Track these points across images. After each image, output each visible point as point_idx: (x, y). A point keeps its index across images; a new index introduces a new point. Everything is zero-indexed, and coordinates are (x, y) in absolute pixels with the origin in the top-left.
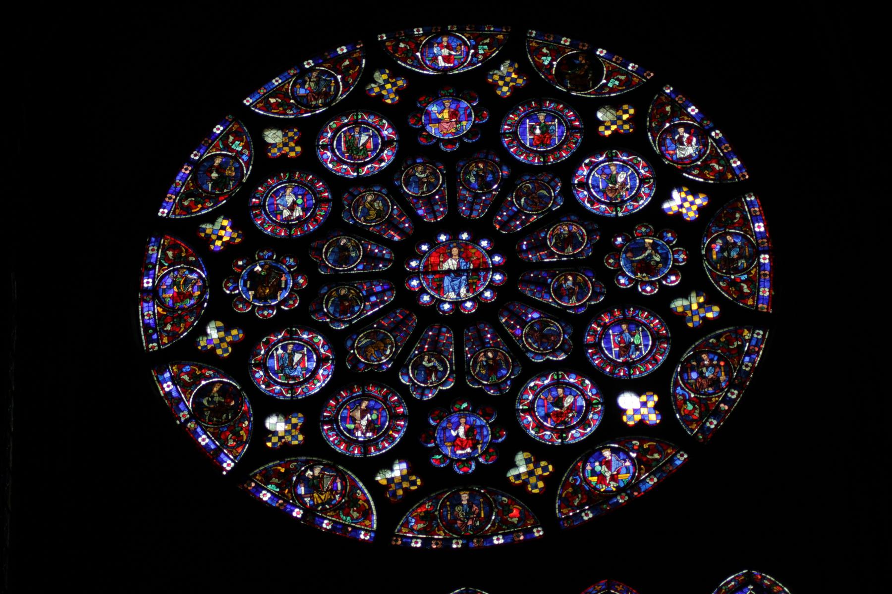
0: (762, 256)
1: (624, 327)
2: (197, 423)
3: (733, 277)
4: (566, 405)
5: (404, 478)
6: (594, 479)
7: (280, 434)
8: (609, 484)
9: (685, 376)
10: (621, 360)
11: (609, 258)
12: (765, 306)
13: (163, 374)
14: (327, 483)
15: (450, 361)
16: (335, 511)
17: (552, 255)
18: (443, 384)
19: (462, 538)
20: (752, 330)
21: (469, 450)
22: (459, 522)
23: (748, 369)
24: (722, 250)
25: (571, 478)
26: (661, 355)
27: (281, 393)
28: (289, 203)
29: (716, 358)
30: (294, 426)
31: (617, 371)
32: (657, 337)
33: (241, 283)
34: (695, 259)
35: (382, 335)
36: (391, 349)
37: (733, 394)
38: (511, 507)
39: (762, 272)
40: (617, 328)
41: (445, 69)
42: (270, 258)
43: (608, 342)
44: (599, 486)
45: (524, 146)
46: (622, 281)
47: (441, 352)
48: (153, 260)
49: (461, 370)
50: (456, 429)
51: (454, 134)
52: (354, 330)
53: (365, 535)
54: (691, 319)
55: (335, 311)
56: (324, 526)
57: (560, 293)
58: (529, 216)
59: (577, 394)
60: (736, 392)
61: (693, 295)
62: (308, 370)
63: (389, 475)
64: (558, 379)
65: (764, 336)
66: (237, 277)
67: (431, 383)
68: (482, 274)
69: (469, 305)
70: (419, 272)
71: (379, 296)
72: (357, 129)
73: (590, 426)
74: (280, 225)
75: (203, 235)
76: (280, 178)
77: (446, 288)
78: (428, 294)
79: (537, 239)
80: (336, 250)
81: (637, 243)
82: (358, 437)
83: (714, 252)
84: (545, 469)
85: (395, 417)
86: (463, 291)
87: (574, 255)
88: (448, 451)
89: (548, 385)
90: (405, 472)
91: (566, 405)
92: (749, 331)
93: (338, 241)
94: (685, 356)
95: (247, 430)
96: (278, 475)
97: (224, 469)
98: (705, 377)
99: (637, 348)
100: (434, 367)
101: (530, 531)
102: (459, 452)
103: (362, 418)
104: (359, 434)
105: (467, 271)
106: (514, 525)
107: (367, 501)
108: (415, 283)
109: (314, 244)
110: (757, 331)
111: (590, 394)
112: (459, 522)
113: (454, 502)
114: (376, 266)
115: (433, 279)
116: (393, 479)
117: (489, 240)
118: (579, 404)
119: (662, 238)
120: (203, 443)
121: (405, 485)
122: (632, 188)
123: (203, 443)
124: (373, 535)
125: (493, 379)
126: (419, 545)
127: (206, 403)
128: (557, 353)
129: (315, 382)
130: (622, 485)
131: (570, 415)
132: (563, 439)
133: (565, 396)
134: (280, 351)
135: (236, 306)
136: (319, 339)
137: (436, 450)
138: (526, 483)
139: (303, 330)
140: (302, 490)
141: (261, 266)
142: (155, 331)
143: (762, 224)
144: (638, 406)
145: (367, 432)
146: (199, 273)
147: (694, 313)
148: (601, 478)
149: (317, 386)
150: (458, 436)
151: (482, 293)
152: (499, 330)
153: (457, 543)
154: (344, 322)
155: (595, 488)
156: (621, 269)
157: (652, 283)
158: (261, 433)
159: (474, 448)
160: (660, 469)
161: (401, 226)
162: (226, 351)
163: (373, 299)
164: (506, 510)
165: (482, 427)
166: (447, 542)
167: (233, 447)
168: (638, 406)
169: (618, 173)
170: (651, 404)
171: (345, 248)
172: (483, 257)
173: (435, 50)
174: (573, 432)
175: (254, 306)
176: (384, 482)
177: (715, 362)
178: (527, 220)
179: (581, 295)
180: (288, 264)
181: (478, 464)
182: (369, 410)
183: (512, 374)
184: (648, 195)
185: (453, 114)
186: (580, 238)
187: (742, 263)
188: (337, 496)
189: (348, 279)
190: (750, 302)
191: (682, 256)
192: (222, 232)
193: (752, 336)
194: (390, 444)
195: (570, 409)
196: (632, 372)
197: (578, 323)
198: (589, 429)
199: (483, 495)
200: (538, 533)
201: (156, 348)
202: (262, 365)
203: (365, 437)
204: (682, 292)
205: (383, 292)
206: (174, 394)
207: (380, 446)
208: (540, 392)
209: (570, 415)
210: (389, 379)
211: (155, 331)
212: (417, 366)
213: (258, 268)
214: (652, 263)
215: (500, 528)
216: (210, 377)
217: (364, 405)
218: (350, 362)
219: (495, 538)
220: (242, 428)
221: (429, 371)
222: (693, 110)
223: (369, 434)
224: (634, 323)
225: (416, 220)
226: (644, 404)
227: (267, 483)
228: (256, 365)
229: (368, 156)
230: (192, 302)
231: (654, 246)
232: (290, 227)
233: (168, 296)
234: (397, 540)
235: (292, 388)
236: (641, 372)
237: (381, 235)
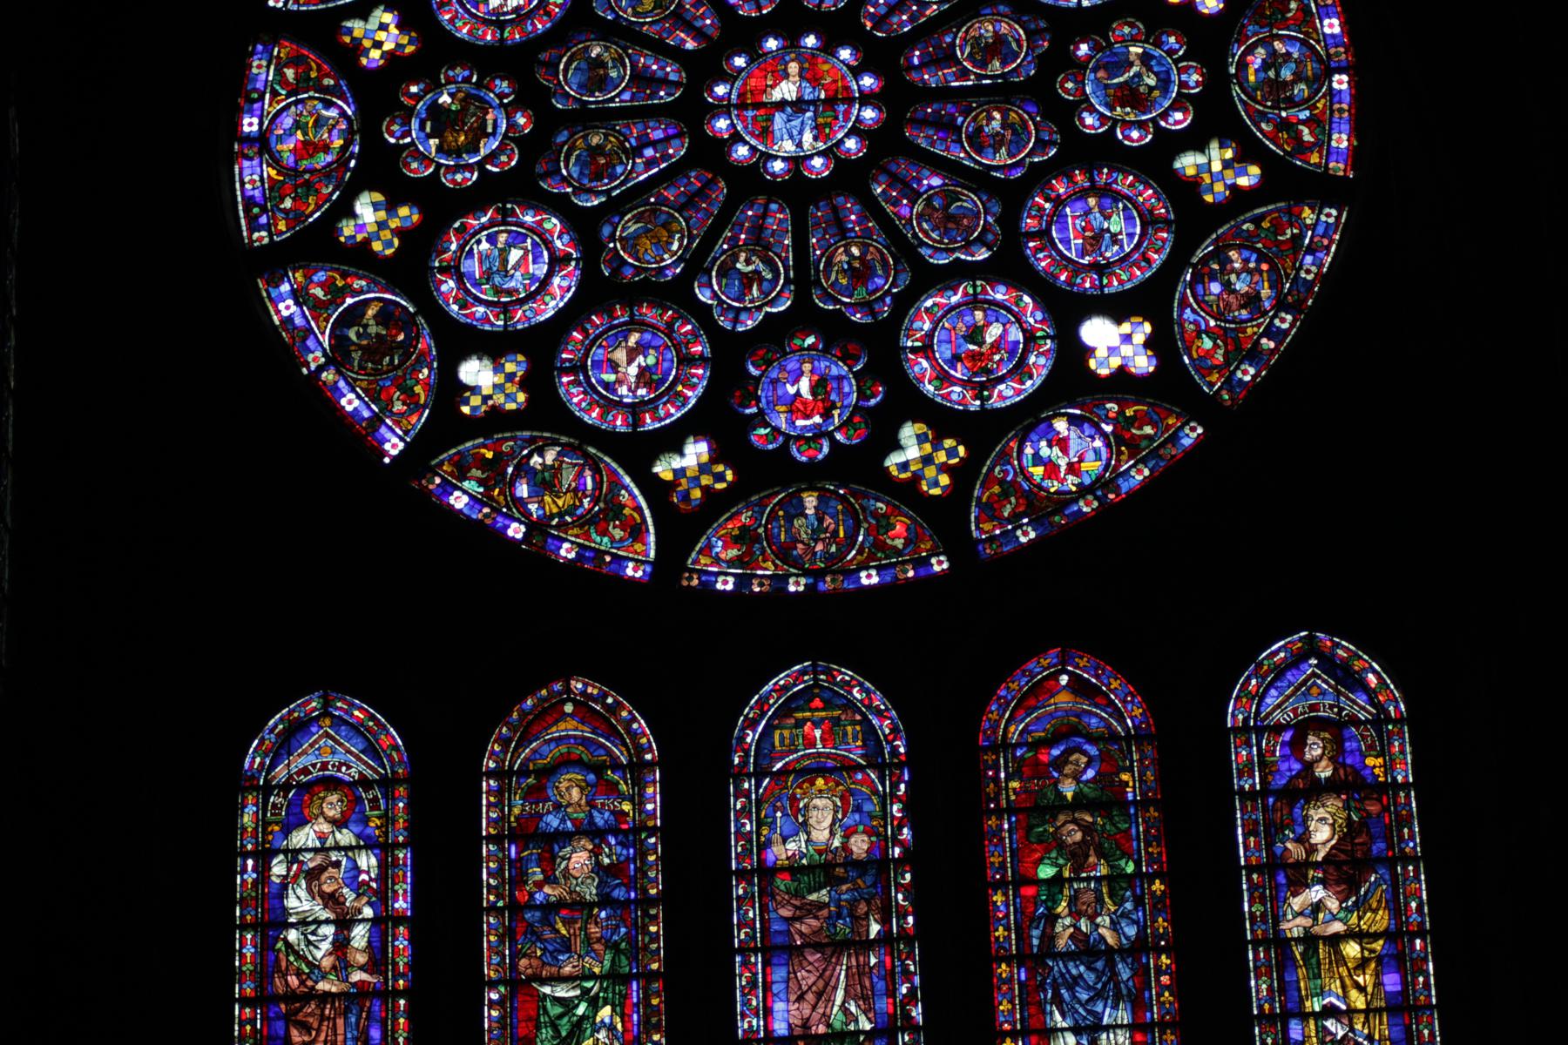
0: (1336, 77)
1: (1092, 201)
2: (339, 372)
3: (1284, 114)
4: (989, 340)
5: (703, 468)
6: (1038, 471)
7: (485, 392)
8: (1065, 479)
9: (1200, 289)
11: (1066, 80)
12: (1342, 166)
13: (278, 286)
14: (568, 477)
15: (784, 261)
16: (581, 526)
17: (965, 74)
18: (771, 303)
19: (806, 573)
20: (1318, 209)
21: (817, 419)
22: (800, 546)
23: (1310, 277)
24: (1265, 66)
25: (997, 469)
26: (1156, 252)
27: (486, 320)
29: (1254, 257)
30: (510, 377)
31: (1079, 281)
32: (1150, 221)
33: (415, 124)
34: (1217, 82)
35: (664, 217)
36: (681, 240)
37: (1283, 320)
38: (892, 520)
39: (1336, 106)
40: (1079, 205)
42: (467, 80)
44: (1047, 483)
46: (1089, 120)
47: (768, 247)
48: (260, 85)
49: (804, 278)
50: (796, 381)
52: (615, 207)
53: (635, 569)
54: (1211, 189)
55: (581, 173)
56: (563, 553)
57: (979, 142)
59: (1009, 321)
60: (1289, 318)
61: (1214, 145)
62: (533, 278)
63: (677, 462)
64: (975, 294)
65: (1338, 218)
66: (409, 112)
67: (752, 301)
68: (842, 108)
69: (817, 162)
70: (729, 105)
71: (659, 147)
73: (1031, 377)
74: (486, 22)
75: (347, 39)
77: (777, 134)
78: (746, 143)
79: (938, 47)
80: (584, 66)
81: (1115, 54)
82: (621, 397)
83: (1251, 71)
84: (952, 453)
85: (686, 360)
86: (808, 137)
87: (1003, 76)
88: (781, 421)
89: (958, 305)
90: (705, 458)
91: (989, 340)
92: (1312, 209)
93: (586, 49)
94: (1200, 254)
95: (426, 384)
96: (482, 463)
97: (385, 453)
98: (1235, 291)
99: (1115, 240)
100: (757, 272)
101: (925, 562)
102: (800, 423)
103: (630, 362)
104: (623, 390)
105: (814, 102)
106: (898, 552)
107: (639, 509)
108: (722, 124)
109: (543, 56)
110: (1327, 210)
111: (1031, 320)
112: (800, 546)
113: (792, 511)
114: (654, 94)
115: (754, 118)
116: (683, 470)
117: (855, 48)
118: (1011, 338)
119: (1158, 44)
120: (349, 408)
121: (706, 480)
123: (349, 408)
124: (648, 569)
125: (861, 293)
126: (730, 587)
127: (354, 338)
128: (974, 248)
129: (547, 299)
130: (1087, 481)
131: (997, 357)
132: (984, 400)
133: (988, 324)
134: (485, 246)
135: (407, 165)
136: (553, 224)
137: (761, 419)
138: (917, 477)
139: (525, 207)
140: (523, 490)
141: (451, 95)
142: (264, 210)
143: (1335, 21)
144: (1116, 342)
145: (637, 387)
146: (340, 108)
147: (1220, 177)
148: (1051, 469)
149: (550, 307)
150: (798, 394)
151: (841, 141)
152: (871, 207)
153: (797, 583)
154: (598, 194)
155: (1039, 486)
156: (1087, 100)
157: (1141, 125)
158: (451, 389)
159: (827, 415)
160: (1154, 453)
161: (698, 24)
162: (389, 244)
163: (649, 152)
164: (883, 524)
165: (840, 378)
166: (780, 580)
167: (402, 414)
168: (1116, 342)
170: (1139, 338)
171: (599, 63)
172: (844, 78)
174: (1002, 387)
175: (439, 166)
176: (668, 476)
177: (1252, 265)
178: (921, 13)
179: (1016, 146)
180: (497, 90)
181: (833, 442)
182: (641, 348)
183: (894, 285)
186: (1014, 45)
187: (1301, 89)
188: (586, 501)
189: (604, 117)
190: (1315, 159)
191: (1195, 77)
192: (381, 34)
193: (1318, 219)
194: (678, 409)
195: (996, 347)
196: (1105, 281)
197: (1011, 195)
198: (1029, 383)
199: (843, 499)
200: (939, 565)
201: (266, 241)
202: (453, 270)
203: (635, 396)
204: (1195, 140)
205: (667, 140)
206: (298, 321)
207: (662, 413)
208: (943, 316)
209: (997, 357)
210: (677, 294)
211: (264, 210)
212: (726, 271)
213: (445, 99)
214: (1142, 89)
215: (872, 557)
216: (361, 292)
217: (633, 339)
218: (608, 263)
219: (863, 574)
220: (418, 381)
221: (748, 280)
223: (642, 392)
224: (1108, 194)
226: (1127, 338)
227: (463, 478)
228: (442, 270)
230: (329, 159)
231: (1145, 58)
233: (286, 148)
234: (690, 579)
235: (506, 309)
236: (1121, 282)
237: (662, 41)
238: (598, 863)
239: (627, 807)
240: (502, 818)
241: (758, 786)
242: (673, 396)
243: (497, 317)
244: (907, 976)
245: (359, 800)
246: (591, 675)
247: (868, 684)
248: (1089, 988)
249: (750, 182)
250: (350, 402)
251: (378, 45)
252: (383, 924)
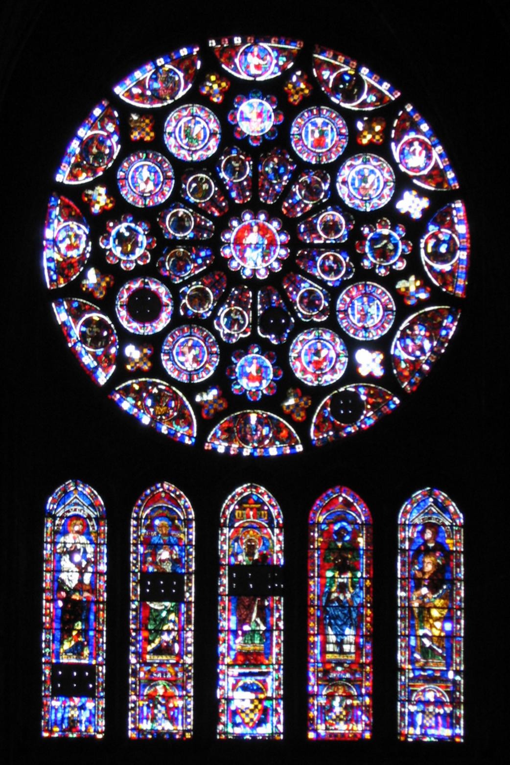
7: (137, 360)
10: (360, 325)
28: (145, 179)
30: (146, 355)
41: (255, 76)
43: (353, 309)
45: (306, 146)
50: (250, 366)
51: (258, 132)
58: (306, 205)
61: (412, 278)
72: (193, 121)
76: (139, 158)
99: (372, 318)
103: (190, 351)
118: (330, 356)
121: (215, 406)
122: (378, 188)
131: (325, 364)
133: (322, 349)
150: (251, 373)
169: (369, 175)
173: (249, 56)
175: (120, 260)
184: (388, 196)
185: (260, 115)
194: (207, 374)
195: (325, 359)
197: (333, 293)
200: (299, 448)
204: (404, 275)
222: (425, 127)
223: (195, 366)
224: (370, 296)
225: (231, 201)
229: (199, 145)
232: (145, 198)
238: (172, 557)
239: (182, 536)
240: (139, 537)
241: (229, 531)
242: (204, 369)
243: (141, 328)
244: (278, 610)
245: (88, 526)
246: (171, 481)
247: (270, 494)
248: (341, 620)
249: (235, 278)
251: (98, 202)
252: (95, 573)
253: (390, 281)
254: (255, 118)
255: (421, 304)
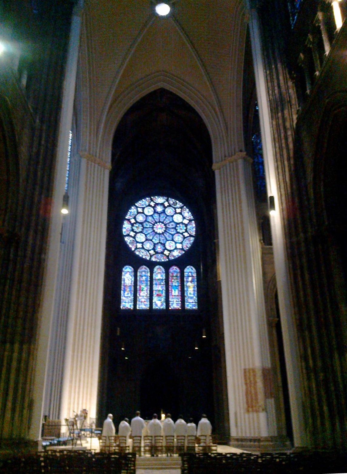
192: (133, 221)
197: (173, 235)
210: (151, 240)
249: (156, 233)
250: (130, 246)
253: (182, 234)
254: (159, 209)
255: (188, 237)
